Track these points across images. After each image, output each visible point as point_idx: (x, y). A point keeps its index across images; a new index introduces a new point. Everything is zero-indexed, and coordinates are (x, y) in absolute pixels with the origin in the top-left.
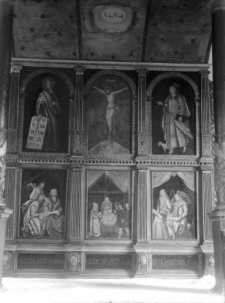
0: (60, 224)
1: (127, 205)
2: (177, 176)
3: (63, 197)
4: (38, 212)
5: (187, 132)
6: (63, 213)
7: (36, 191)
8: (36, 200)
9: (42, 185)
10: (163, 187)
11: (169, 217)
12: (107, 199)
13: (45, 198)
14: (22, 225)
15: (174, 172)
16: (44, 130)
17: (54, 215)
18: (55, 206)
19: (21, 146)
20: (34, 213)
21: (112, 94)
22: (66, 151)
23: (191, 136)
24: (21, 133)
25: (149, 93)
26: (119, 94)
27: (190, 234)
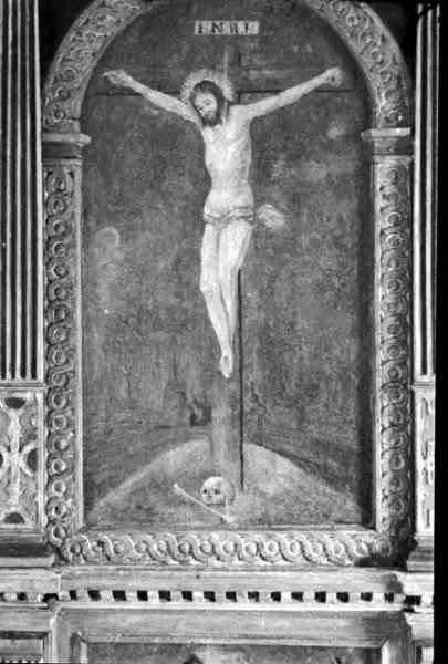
21: (240, 116)
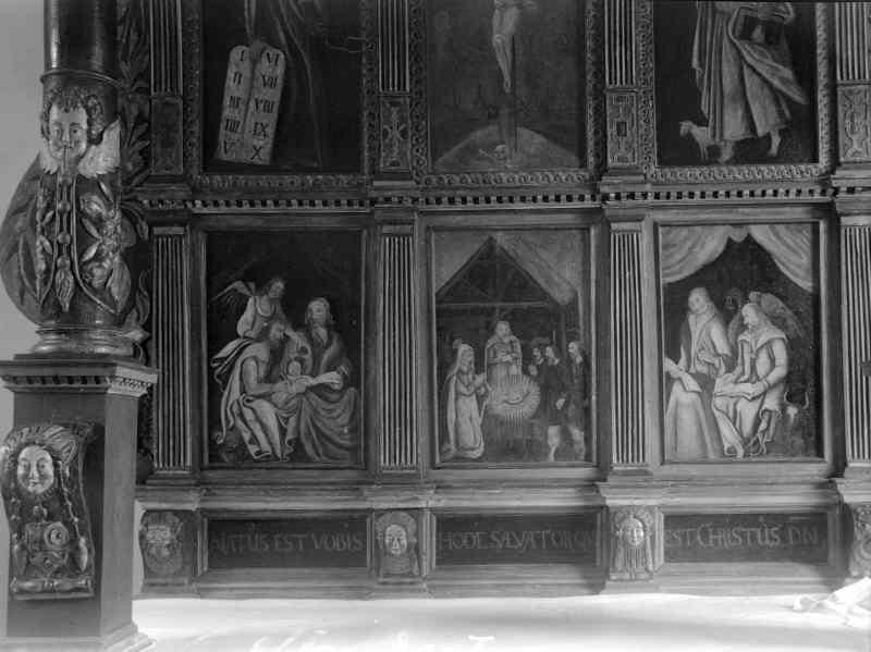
0: (344, 419)
1: (573, 347)
2: (749, 239)
3: (350, 327)
4: (269, 378)
5: (784, 80)
6: (352, 380)
7: (256, 310)
8: (258, 340)
10: (699, 278)
11: (722, 385)
12: (503, 328)
13: (290, 333)
14: (215, 422)
15: (737, 225)
16: (274, 95)
17: (322, 390)
18: (326, 357)
19: (196, 153)
20: (252, 379)
22: (355, 168)
23: (797, 96)
24: (197, 107)
27: (799, 441)
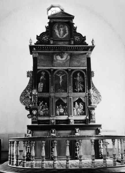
2: (80, 98)
3: (48, 106)
4: (42, 109)
6: (49, 109)
9: (43, 102)
10: (76, 101)
11: (78, 110)
16: (42, 86)
21: (61, 76)
25: (72, 76)
26: (63, 76)
